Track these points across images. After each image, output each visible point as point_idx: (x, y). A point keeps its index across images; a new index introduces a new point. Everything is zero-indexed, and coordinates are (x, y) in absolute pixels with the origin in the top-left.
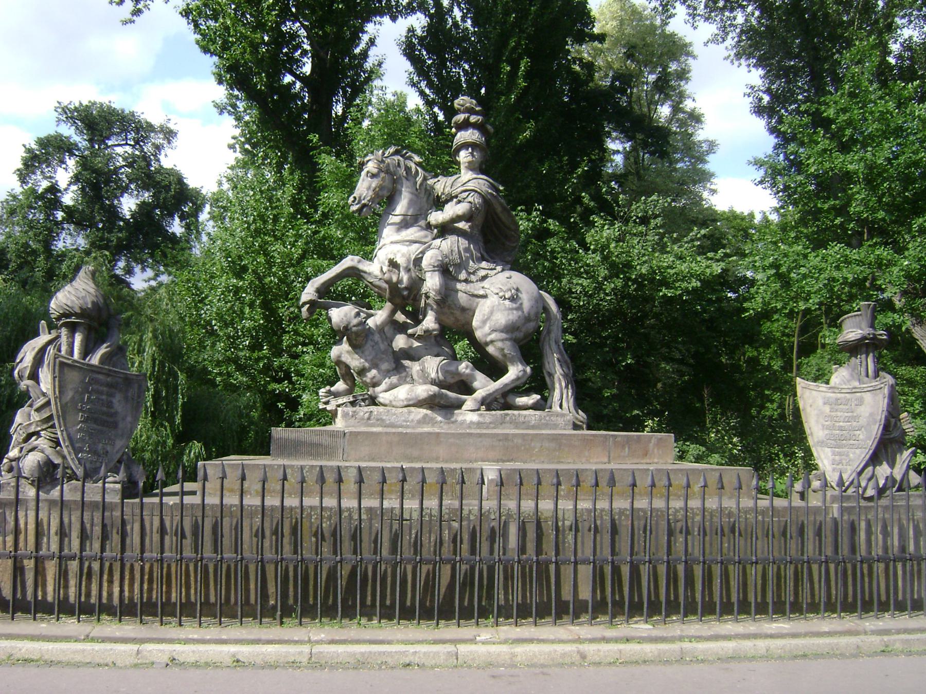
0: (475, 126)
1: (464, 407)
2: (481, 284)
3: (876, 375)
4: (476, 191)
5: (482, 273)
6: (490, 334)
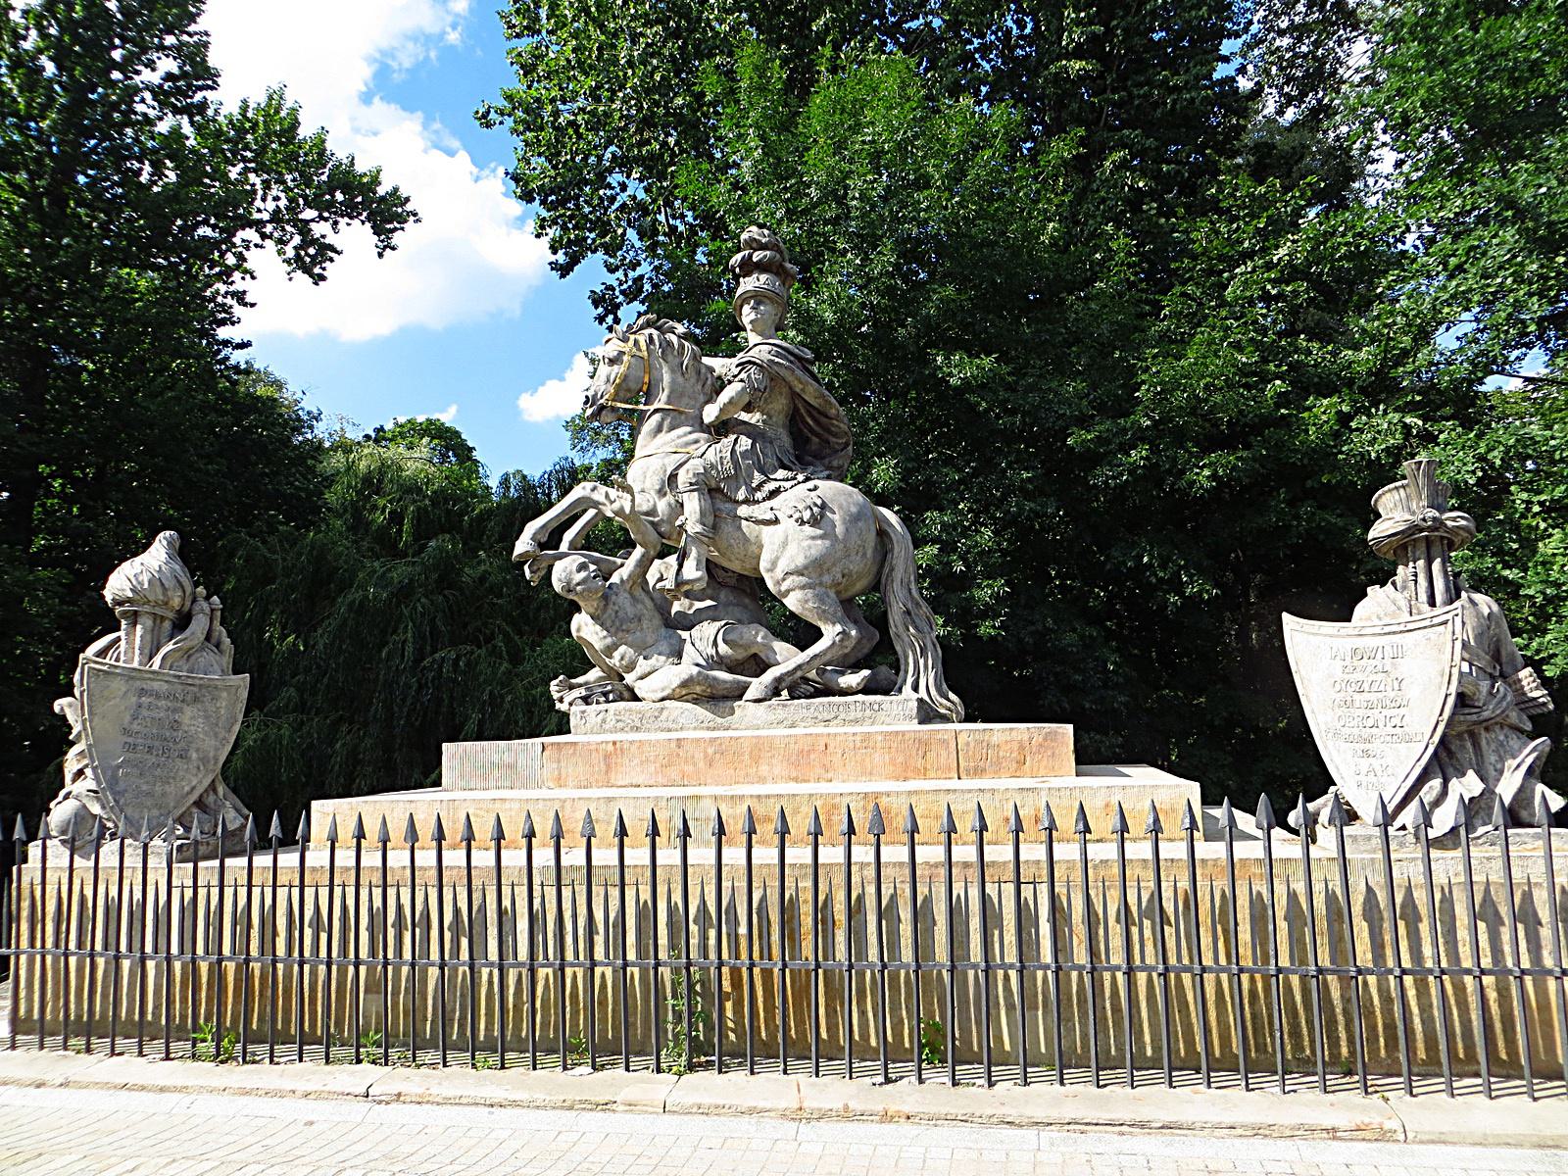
0: (762, 267)
1: (748, 695)
2: (768, 504)
3: (1453, 595)
4: (754, 363)
5: (772, 486)
6: (784, 580)
